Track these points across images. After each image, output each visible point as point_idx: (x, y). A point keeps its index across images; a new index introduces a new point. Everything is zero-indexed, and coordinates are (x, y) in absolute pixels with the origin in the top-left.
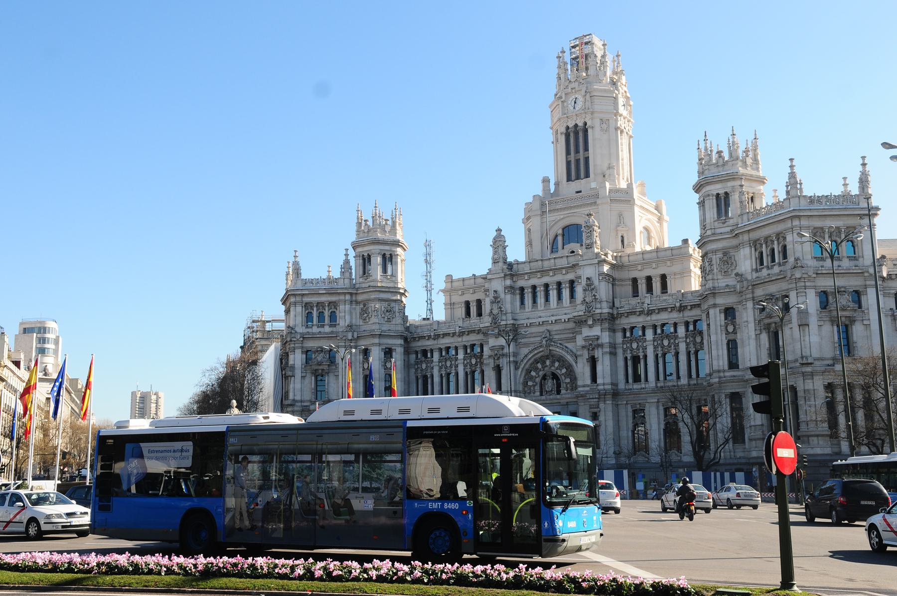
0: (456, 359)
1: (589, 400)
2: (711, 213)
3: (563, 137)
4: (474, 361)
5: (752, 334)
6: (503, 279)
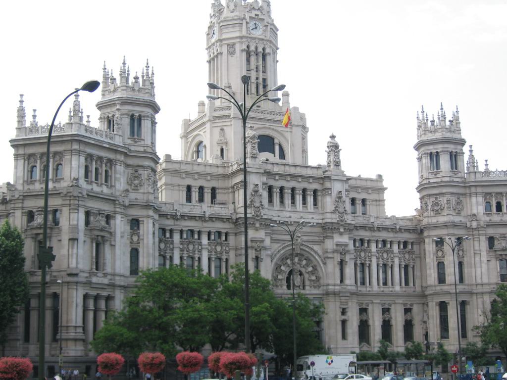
0: (200, 244)
1: (342, 298)
2: (445, 163)
3: (244, 54)
4: (219, 248)
5: (484, 258)
6: (261, 175)
